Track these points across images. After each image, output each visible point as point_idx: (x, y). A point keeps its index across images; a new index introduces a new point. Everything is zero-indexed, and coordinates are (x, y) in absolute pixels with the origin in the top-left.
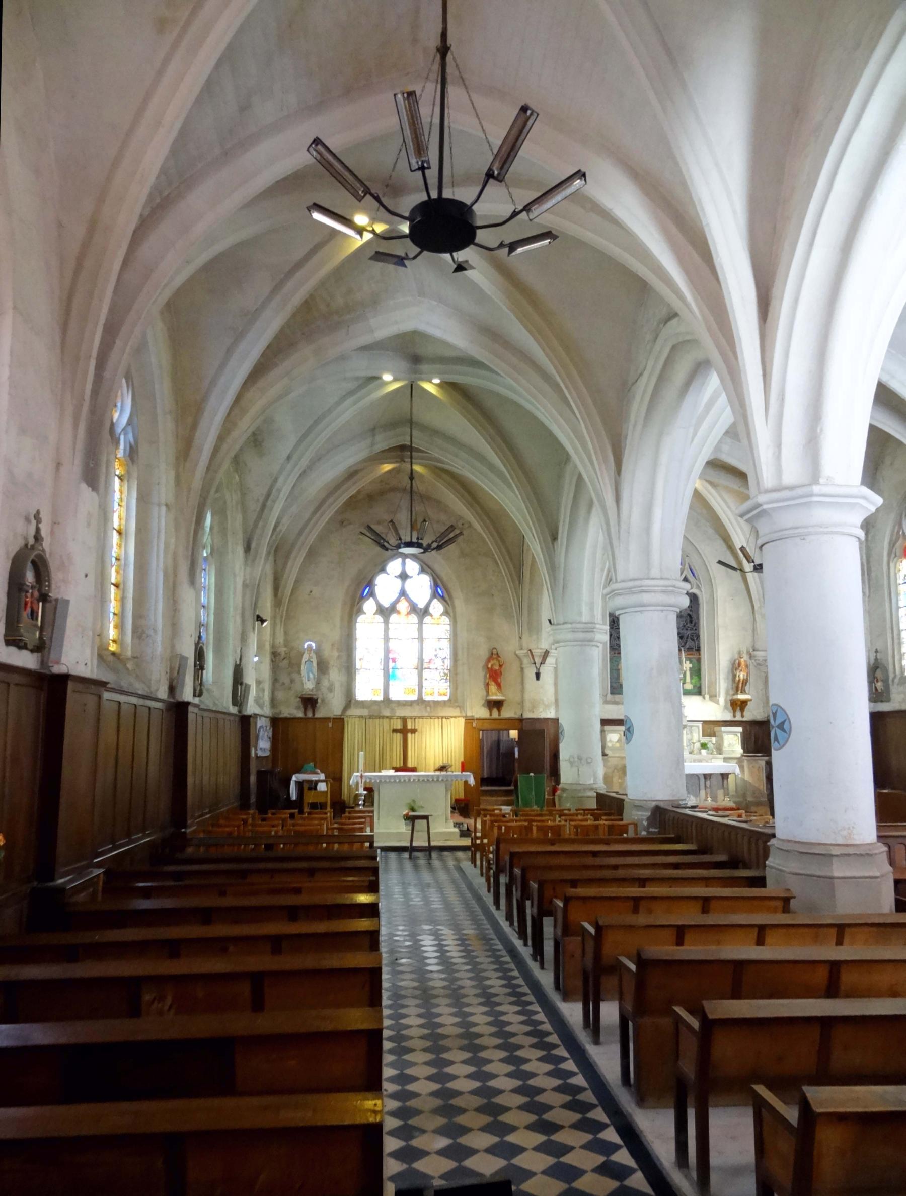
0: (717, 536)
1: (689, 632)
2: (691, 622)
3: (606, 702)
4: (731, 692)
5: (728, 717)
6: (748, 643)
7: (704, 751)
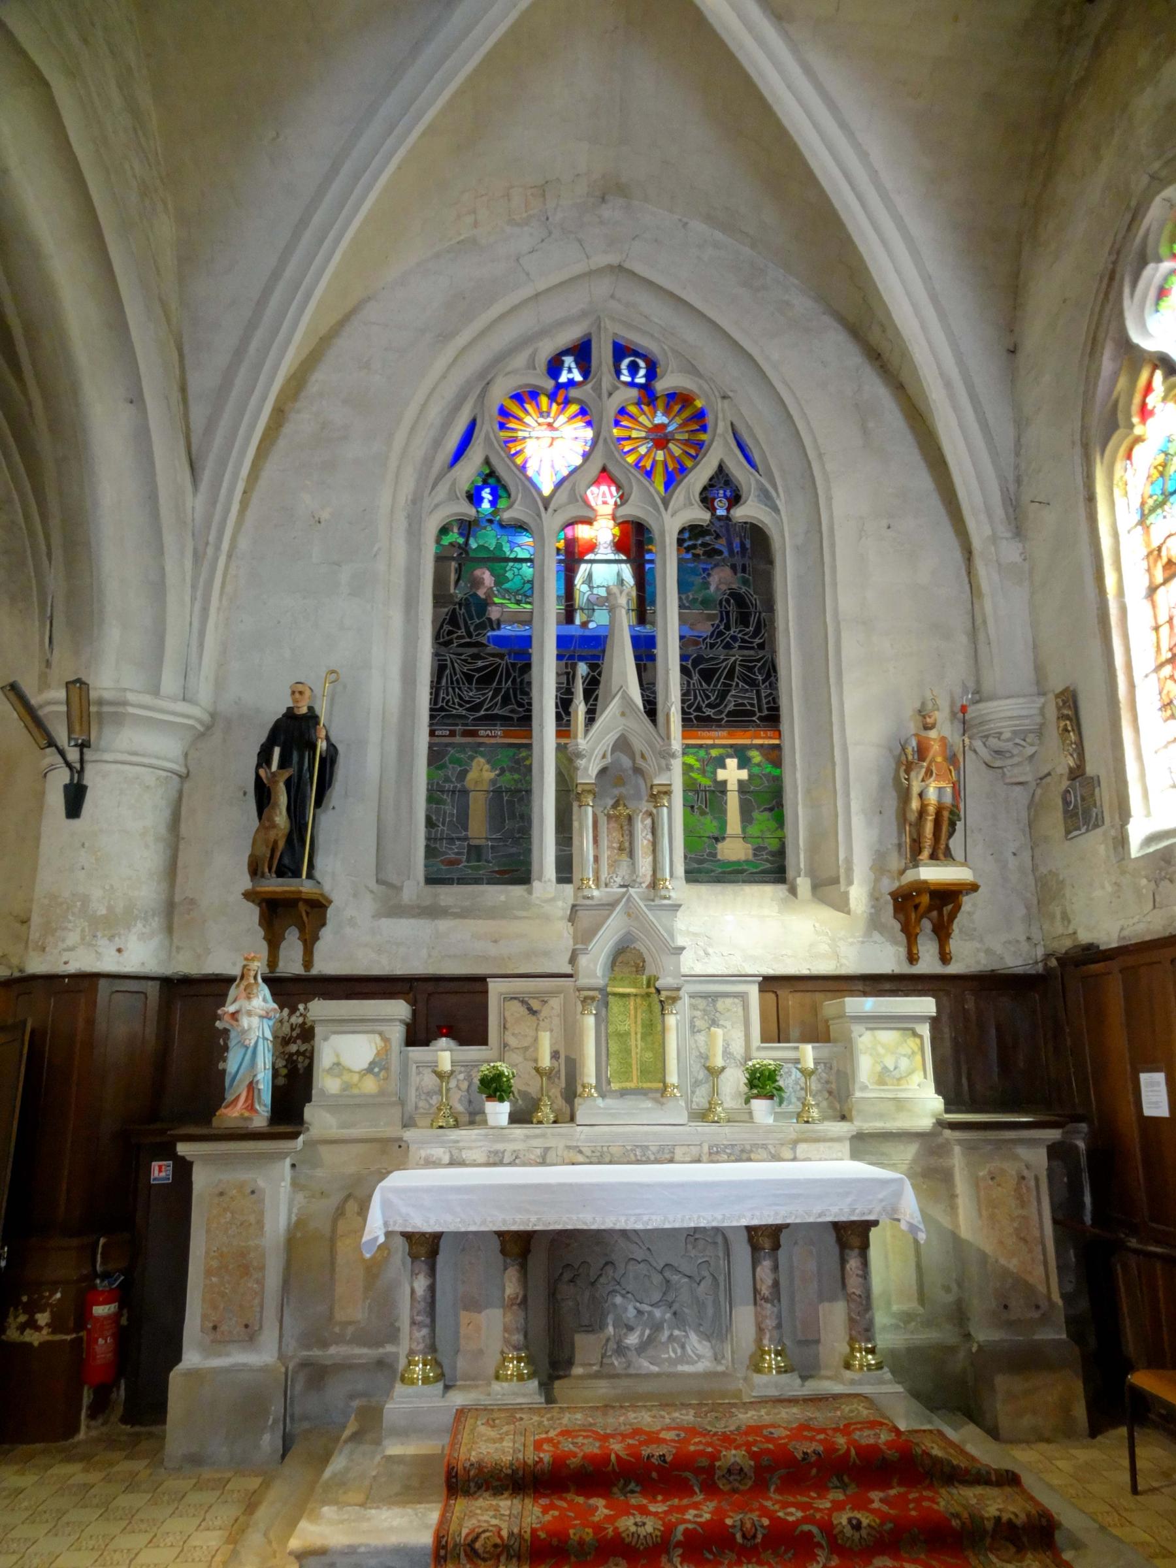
0: (827, 320)
1: (736, 656)
2: (744, 620)
3: (395, 910)
4: (895, 862)
5: (887, 958)
6: (956, 674)
7: (760, 1106)
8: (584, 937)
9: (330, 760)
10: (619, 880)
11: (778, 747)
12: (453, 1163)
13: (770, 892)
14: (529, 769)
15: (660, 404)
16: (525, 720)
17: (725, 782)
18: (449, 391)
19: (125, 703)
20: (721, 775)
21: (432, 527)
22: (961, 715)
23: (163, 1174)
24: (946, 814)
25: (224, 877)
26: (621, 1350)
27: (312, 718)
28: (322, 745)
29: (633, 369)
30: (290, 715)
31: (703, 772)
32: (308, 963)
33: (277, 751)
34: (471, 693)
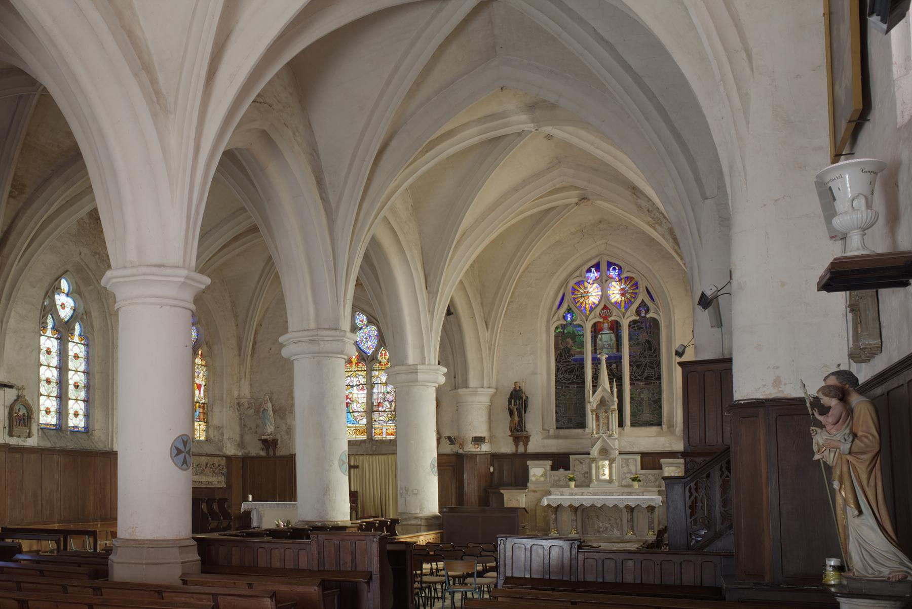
3: (548, 437)
16: (583, 382)
18: (556, 286)
21: (553, 328)
26: (598, 532)
34: (567, 376)
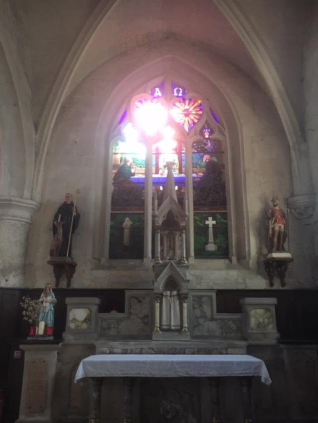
3: (99, 267)
4: (265, 251)
8: (157, 276)
9: (78, 217)
10: (169, 258)
11: (226, 213)
12: (111, 353)
13: (221, 263)
14: (143, 221)
15: (187, 102)
17: (208, 225)
19: (11, 200)
20: (207, 222)
22: (288, 203)
23: (18, 355)
24: (282, 235)
25: (42, 256)
27: (72, 204)
28: (74, 214)
29: (178, 91)
30: (65, 204)
31: (201, 222)
32: (69, 284)
33: (60, 216)
